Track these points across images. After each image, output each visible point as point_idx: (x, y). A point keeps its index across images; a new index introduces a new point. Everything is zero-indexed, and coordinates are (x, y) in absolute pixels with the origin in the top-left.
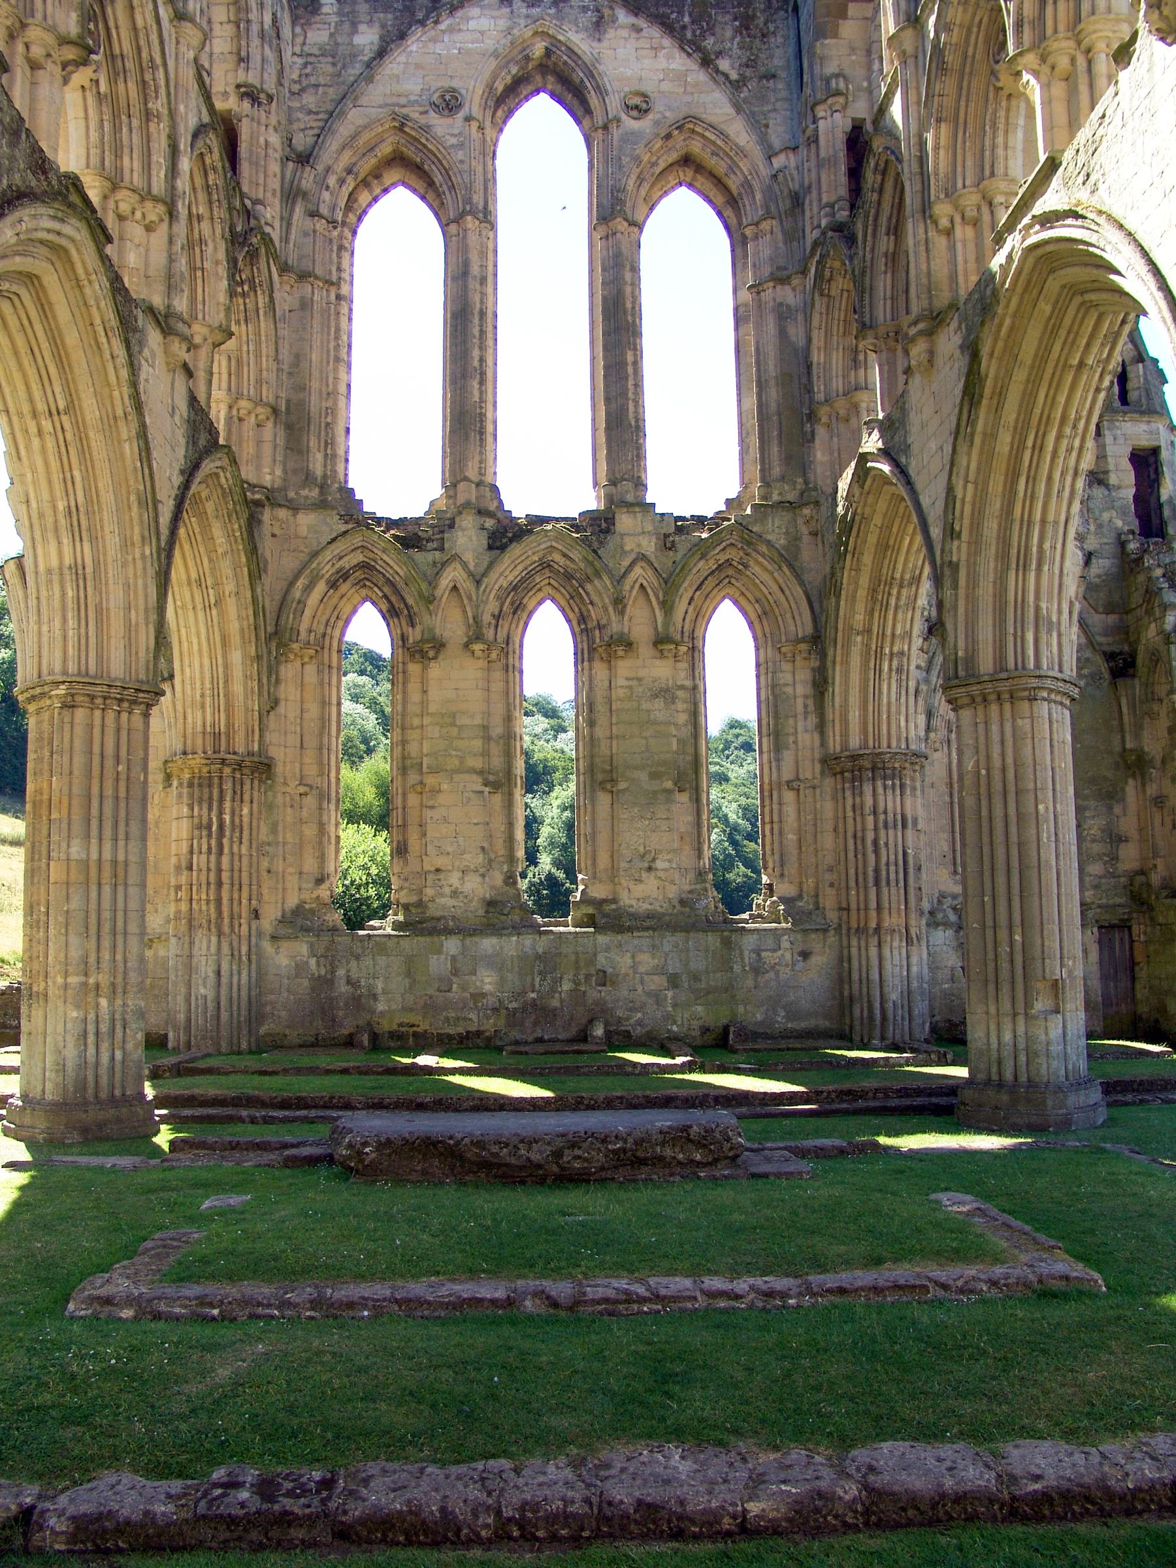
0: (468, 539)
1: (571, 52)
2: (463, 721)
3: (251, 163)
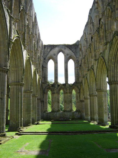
0: (56, 86)
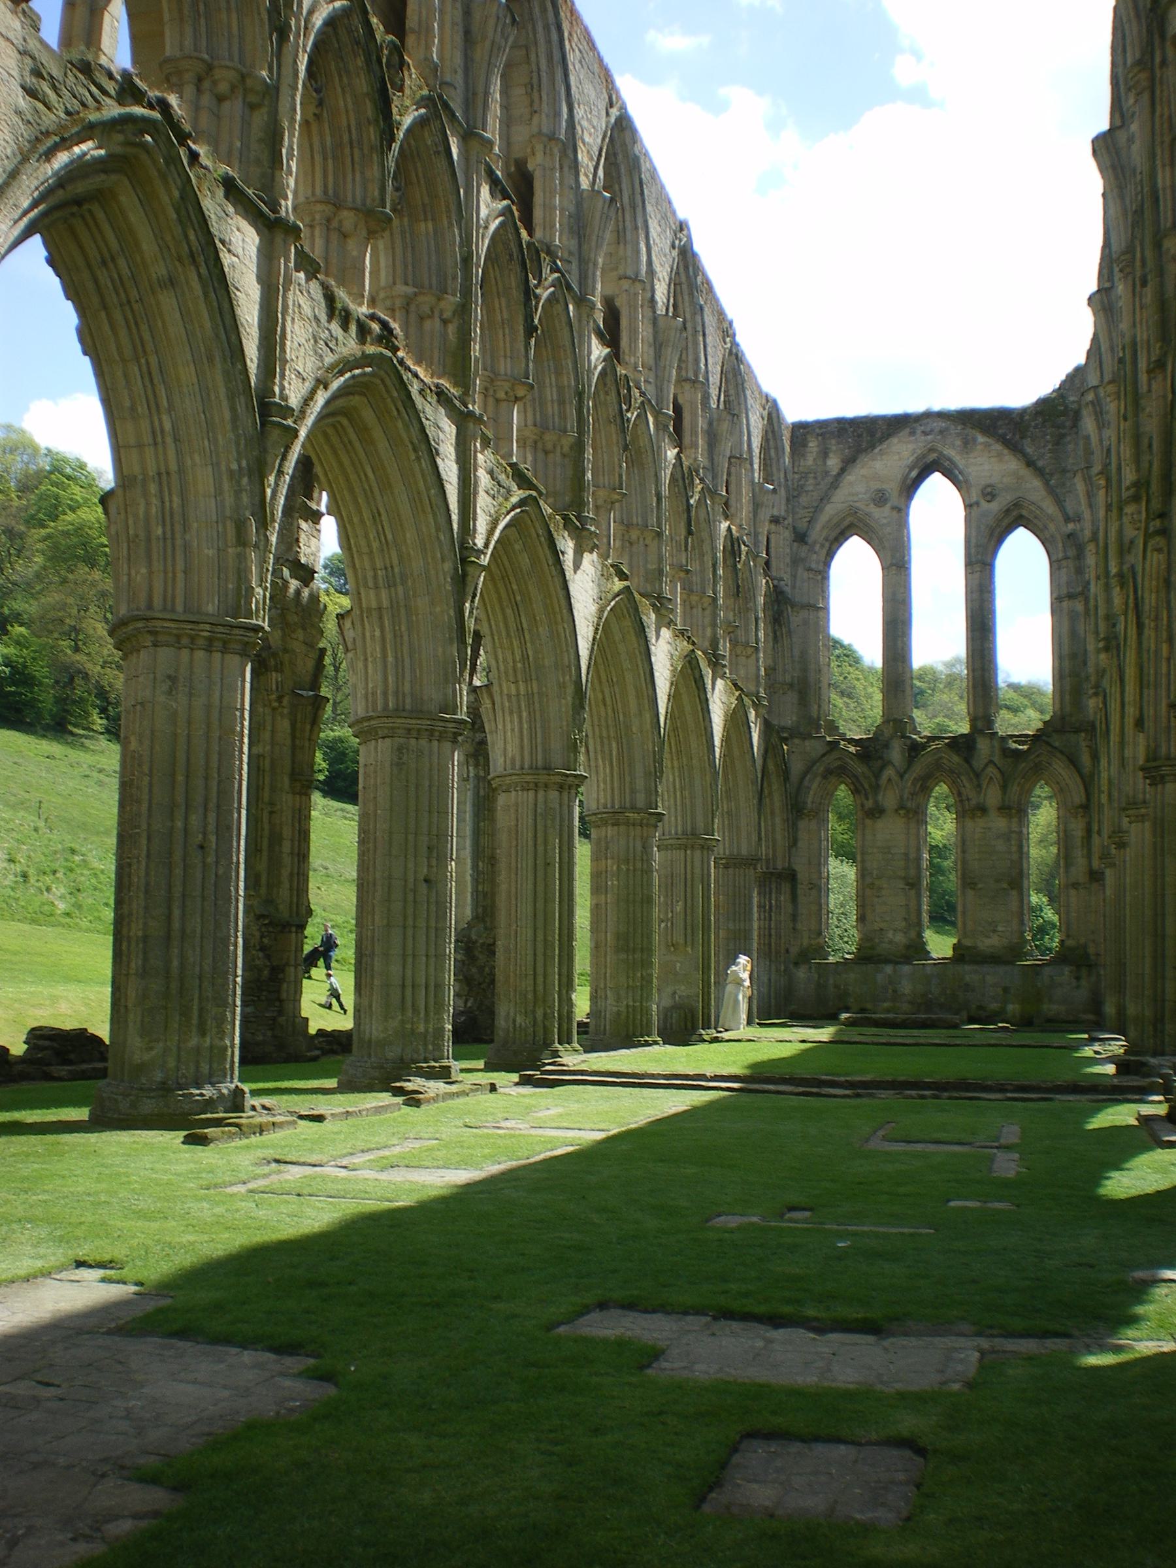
0: (896, 754)
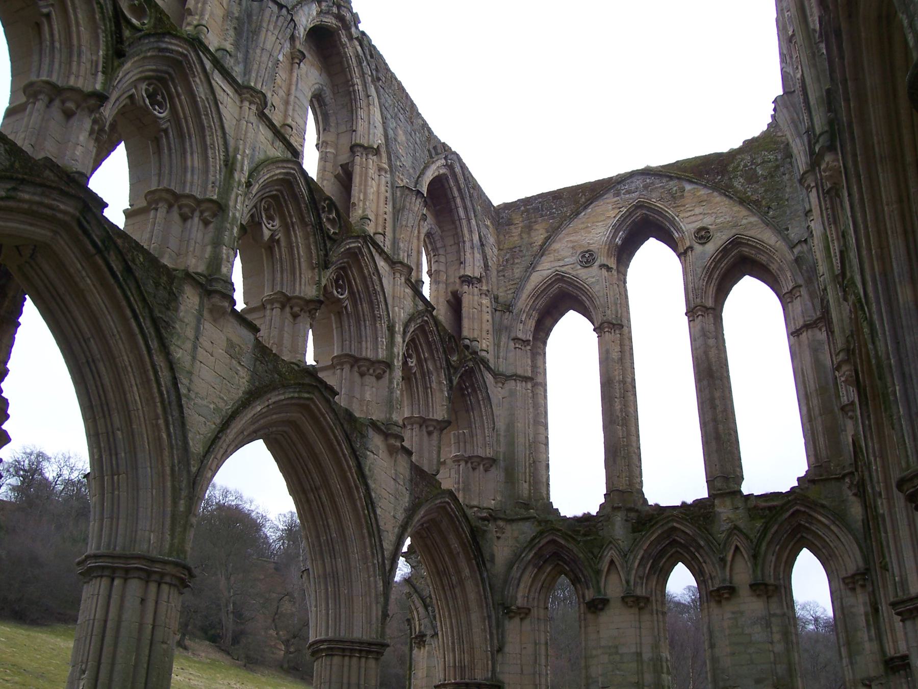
0: (619, 529)
1: (660, 213)
2: (623, 650)
3: (469, 319)
